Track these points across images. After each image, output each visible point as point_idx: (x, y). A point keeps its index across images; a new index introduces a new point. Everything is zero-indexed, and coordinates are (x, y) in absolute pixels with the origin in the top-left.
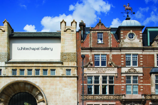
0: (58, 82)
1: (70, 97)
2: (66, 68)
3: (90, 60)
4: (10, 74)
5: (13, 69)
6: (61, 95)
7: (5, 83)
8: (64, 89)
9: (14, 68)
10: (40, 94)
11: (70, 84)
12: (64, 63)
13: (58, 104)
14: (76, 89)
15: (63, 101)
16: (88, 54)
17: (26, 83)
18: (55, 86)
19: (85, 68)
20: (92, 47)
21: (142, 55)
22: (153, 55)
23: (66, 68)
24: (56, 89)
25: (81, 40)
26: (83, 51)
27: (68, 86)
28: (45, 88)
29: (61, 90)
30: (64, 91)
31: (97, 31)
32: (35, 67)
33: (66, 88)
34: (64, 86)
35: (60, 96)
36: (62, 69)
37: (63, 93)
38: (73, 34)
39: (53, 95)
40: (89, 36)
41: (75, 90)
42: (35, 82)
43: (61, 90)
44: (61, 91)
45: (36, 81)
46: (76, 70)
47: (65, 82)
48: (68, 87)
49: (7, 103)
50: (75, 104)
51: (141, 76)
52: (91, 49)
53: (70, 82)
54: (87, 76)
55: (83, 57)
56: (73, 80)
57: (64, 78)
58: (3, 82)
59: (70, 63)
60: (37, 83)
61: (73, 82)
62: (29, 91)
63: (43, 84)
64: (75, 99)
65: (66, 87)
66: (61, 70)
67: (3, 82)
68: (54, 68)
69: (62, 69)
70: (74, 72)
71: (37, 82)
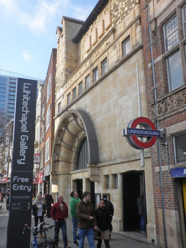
35: (115, 126)
49: (72, 164)
65: (123, 95)
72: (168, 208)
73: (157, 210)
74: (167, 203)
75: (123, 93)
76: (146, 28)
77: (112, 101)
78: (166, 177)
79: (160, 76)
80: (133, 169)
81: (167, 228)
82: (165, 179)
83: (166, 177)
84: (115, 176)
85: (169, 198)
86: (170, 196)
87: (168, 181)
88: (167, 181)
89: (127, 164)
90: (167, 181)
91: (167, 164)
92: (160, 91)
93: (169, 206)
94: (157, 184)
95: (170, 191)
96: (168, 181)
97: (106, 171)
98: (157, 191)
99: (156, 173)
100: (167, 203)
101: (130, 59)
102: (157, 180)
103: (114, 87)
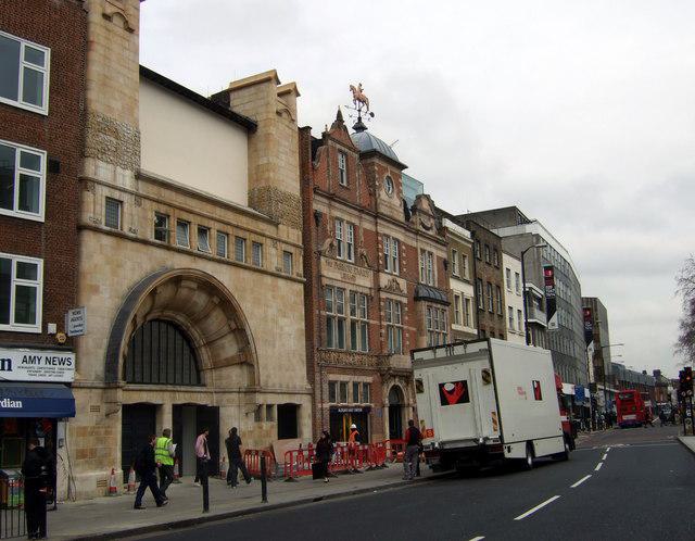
0: (269, 295)
4: (151, 237)
6: (278, 344)
9: (163, 209)
10: (239, 331)
12: (280, 226)
14: (302, 325)
15: (280, 368)
17: (209, 286)
19: (323, 259)
21: (407, 246)
22: (416, 249)
23: (284, 247)
31: (338, 146)
33: (286, 320)
35: (274, 346)
37: (281, 335)
46: (301, 261)
47: (283, 297)
51: (406, 305)
52: (331, 197)
55: (317, 216)
57: (281, 282)
58: (129, 264)
62: (190, 315)
66: (273, 251)
70: (298, 268)
84: (269, 407)
89: (285, 396)
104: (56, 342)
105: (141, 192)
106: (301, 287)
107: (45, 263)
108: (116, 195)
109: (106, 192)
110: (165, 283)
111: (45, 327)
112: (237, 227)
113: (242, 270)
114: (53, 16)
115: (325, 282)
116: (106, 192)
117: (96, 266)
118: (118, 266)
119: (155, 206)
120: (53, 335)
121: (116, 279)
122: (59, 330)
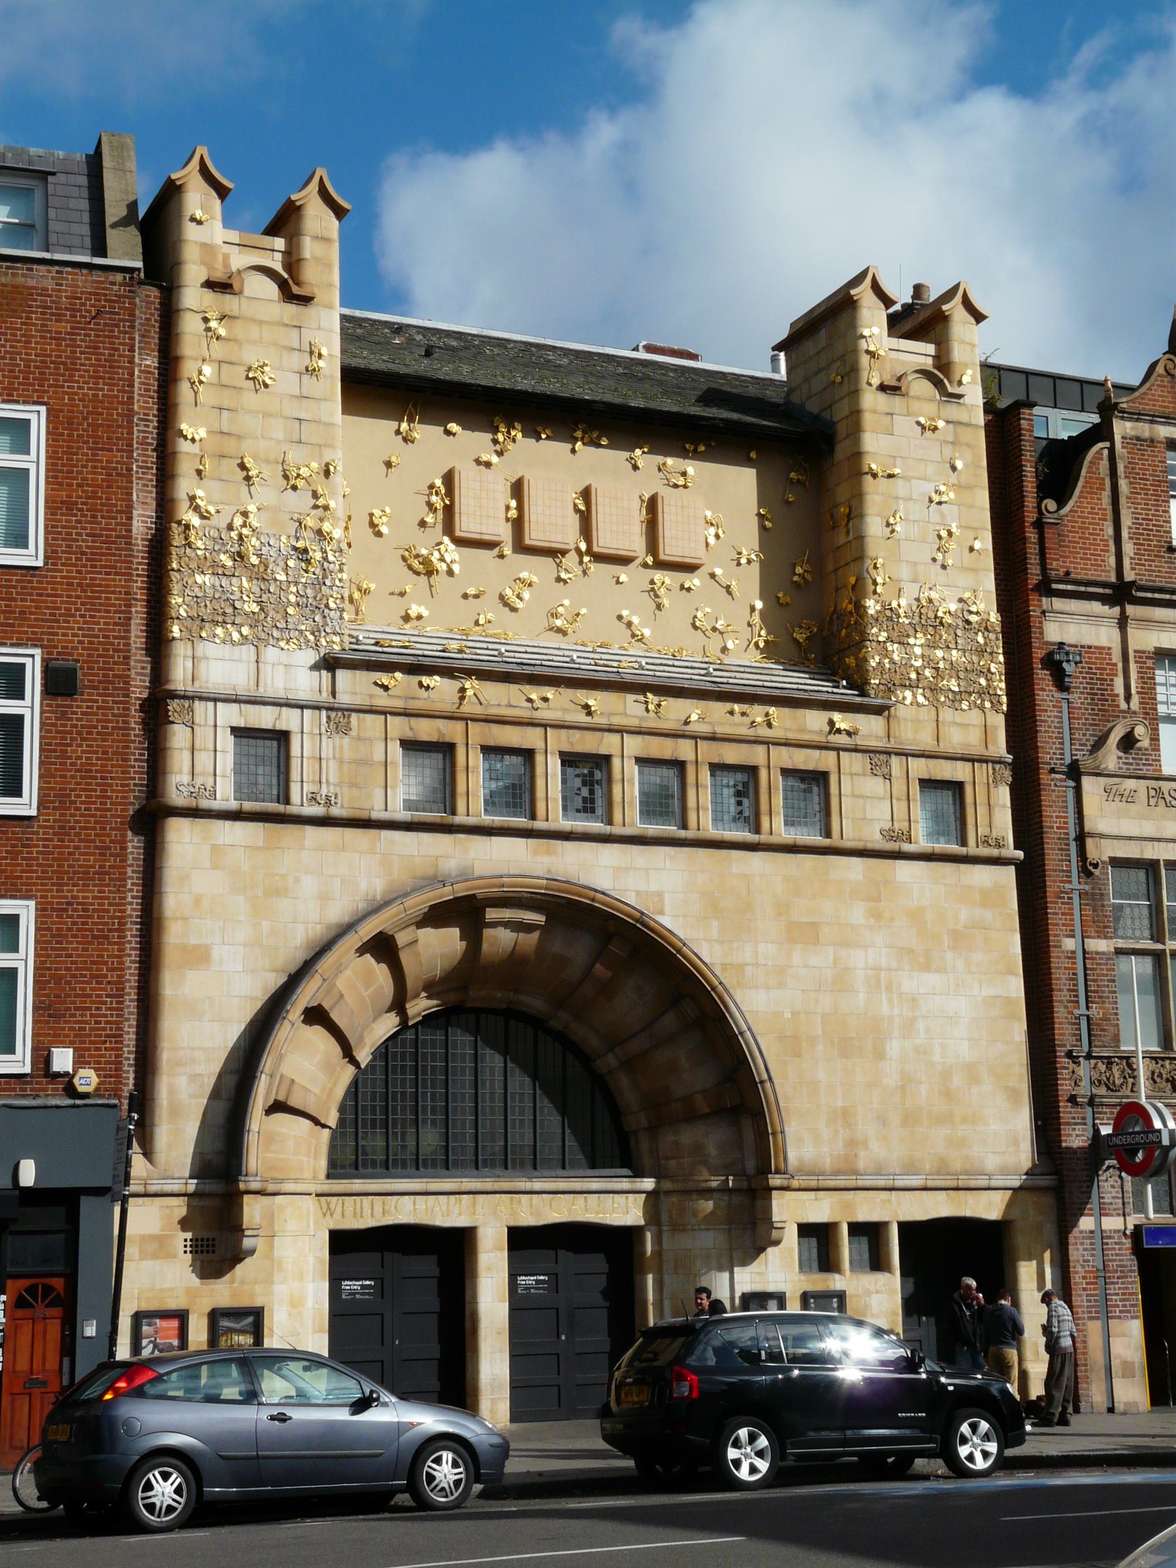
0: (857, 913)
1: (972, 1074)
2: (920, 768)
3: (1124, 706)
5: (409, 735)
6: (894, 1048)
7: (324, 898)
8: (912, 982)
11: (960, 939)
12: (901, 711)
13: (865, 1143)
14: (1016, 987)
16: (1103, 641)
18: (831, 950)
20: (1129, 576)
24: (841, 982)
25: (1040, 500)
26: (1058, 603)
27: (949, 955)
28: (741, 967)
29: (889, 989)
30: (914, 1001)
32: (639, 739)
33: (933, 980)
34: (911, 951)
35: (880, 1055)
36: (888, 777)
37: (909, 1026)
38: (960, 429)
39: (820, 1047)
40: (1104, 464)
41: (1008, 1001)
42: (638, 893)
43: (889, 989)
44: (890, 1001)
45: (654, 887)
46: (1003, 795)
47: (916, 916)
48: (942, 970)
50: (1016, 1143)
53: (964, 915)
54: (1105, 858)
56: (988, 897)
57: (904, 869)
58: (309, 885)
59: (947, 714)
60: (662, 912)
61: (988, 915)
63: (715, 924)
64: (1013, 1094)
65: (927, 967)
66: (876, 786)
67: (309, 885)
68: (816, 753)
69: (888, 777)
71: (660, 895)
72: (1119, 1317)
73: (1084, 1324)
74: (1117, 1306)
75: (922, 960)
76: (1058, 828)
77: (858, 959)
78: (1116, 1243)
79: (1103, 992)
80: (968, 1213)
81: (1115, 1363)
82: (1114, 1249)
83: (1116, 1243)
85: (1124, 1294)
86: (1127, 1288)
87: (1122, 1255)
88: (1117, 1255)
90: (1117, 1255)
91: (1118, 1215)
92: (1104, 1030)
93: (1121, 1312)
94: (1088, 1261)
95: (1126, 1277)
96: (1122, 1255)
97: (820, 1210)
98: (1084, 1278)
99: (1081, 1232)
100: (1117, 1306)
101: (963, 867)
102: (1085, 1250)
103: (877, 915)
104: (70, 1090)
105: (344, 698)
106: (1009, 875)
107: (42, 913)
108: (265, 718)
109: (230, 715)
110: (437, 916)
111: (42, 1059)
112: (713, 738)
113: (735, 854)
114: (53, 326)
115: (1099, 851)
116: (230, 715)
117: (198, 900)
118: (277, 892)
119: (398, 727)
120: (68, 1077)
121: (265, 924)
122: (79, 1062)
